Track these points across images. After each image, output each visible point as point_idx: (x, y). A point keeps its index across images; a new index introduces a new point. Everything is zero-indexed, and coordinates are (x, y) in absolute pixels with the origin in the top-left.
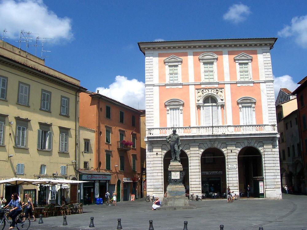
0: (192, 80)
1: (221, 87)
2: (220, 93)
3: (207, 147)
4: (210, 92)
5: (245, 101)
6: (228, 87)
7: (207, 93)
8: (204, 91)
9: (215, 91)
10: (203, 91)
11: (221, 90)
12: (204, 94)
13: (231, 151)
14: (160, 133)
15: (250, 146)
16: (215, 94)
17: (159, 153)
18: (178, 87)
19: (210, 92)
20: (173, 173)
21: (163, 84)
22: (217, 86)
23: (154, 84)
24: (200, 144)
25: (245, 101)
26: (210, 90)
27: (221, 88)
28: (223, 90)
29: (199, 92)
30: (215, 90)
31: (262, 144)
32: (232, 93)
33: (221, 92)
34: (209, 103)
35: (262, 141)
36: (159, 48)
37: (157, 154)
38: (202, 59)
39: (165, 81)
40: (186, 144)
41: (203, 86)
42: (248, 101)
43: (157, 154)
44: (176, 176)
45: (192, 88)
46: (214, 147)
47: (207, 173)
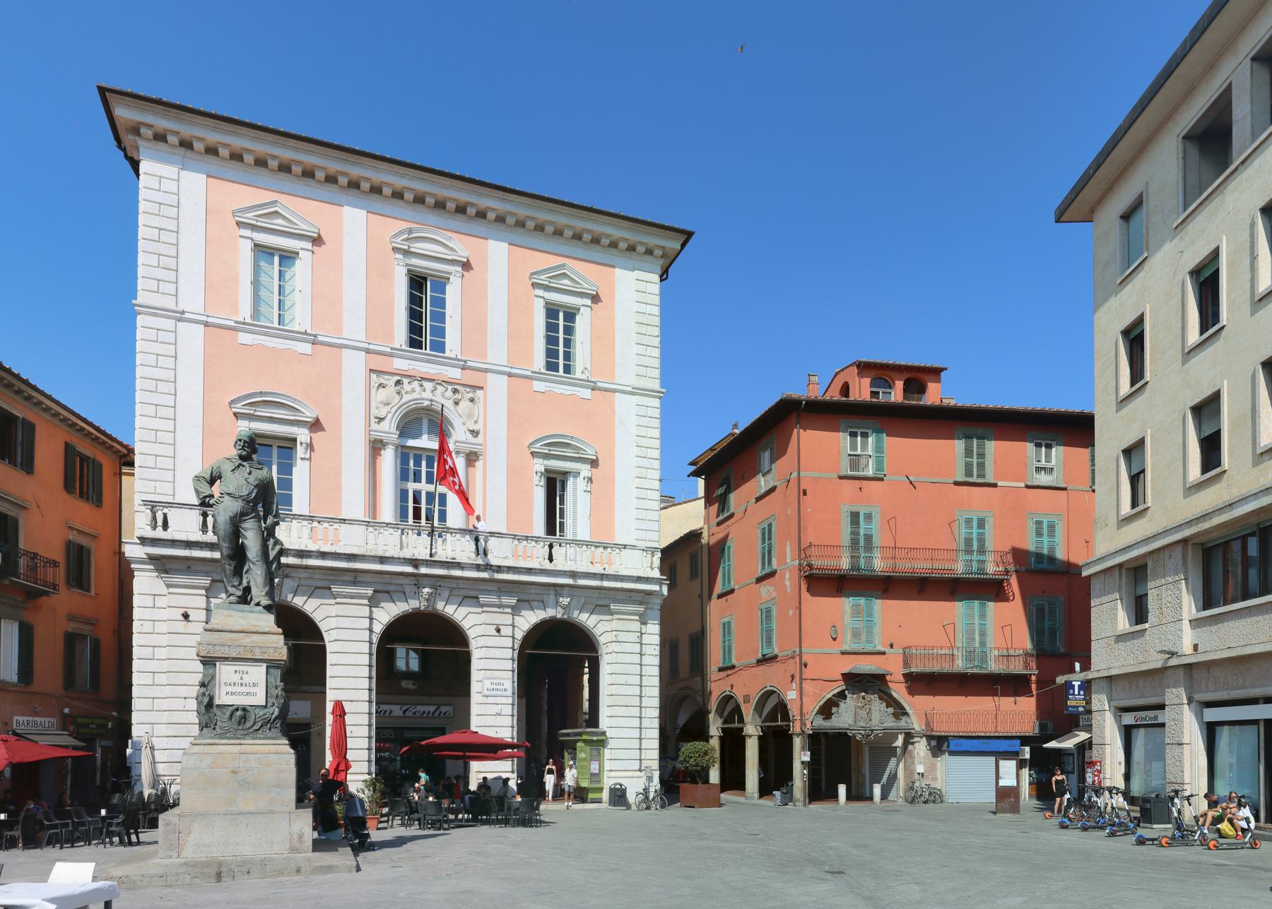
2: (464, 404)
5: (556, 451)
6: (497, 387)
7: (415, 396)
8: (406, 385)
9: (449, 393)
10: (398, 383)
11: (471, 395)
12: (406, 398)
13: (498, 631)
16: (449, 404)
19: (428, 395)
22: (455, 374)
23: (180, 308)
25: (556, 451)
26: (428, 386)
28: (479, 393)
29: (381, 386)
30: (450, 388)
32: (511, 413)
33: (472, 400)
38: (407, 253)
39: (235, 307)
45: (354, 365)
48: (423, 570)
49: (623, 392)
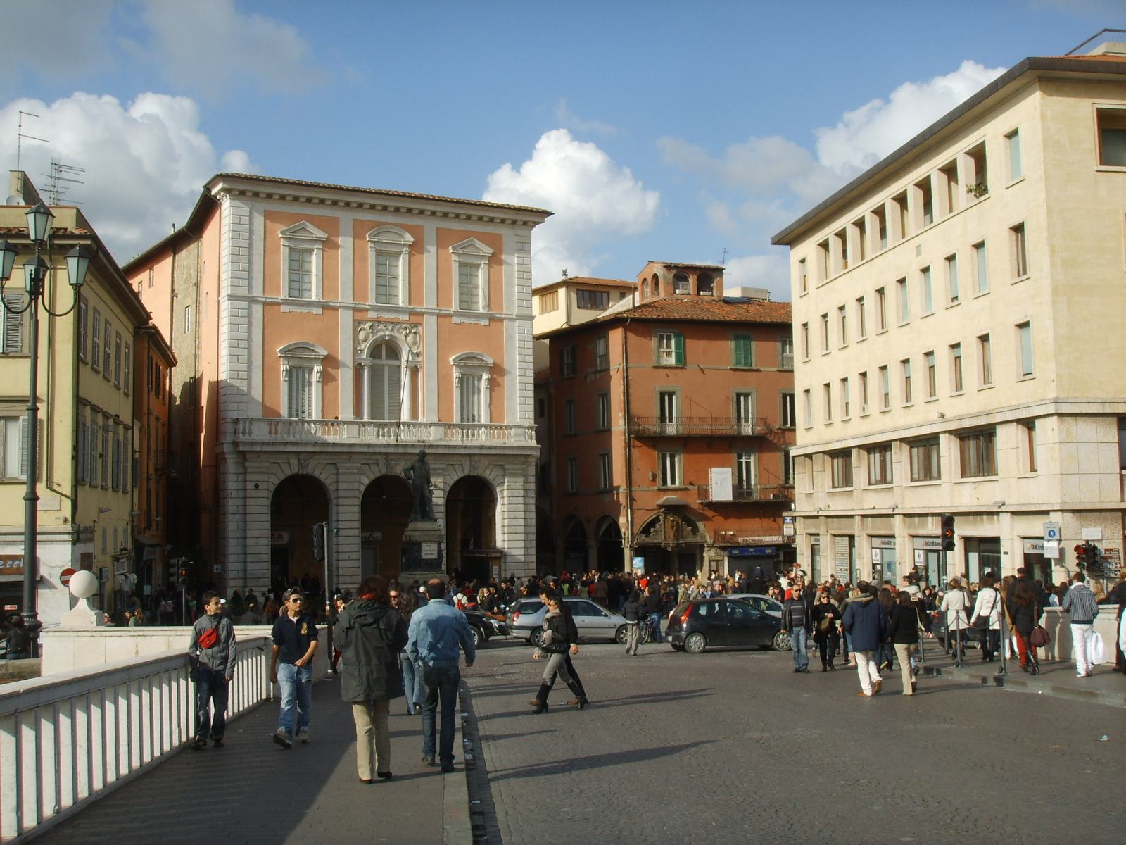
0: (344, 296)
1: (415, 317)
3: (378, 474)
4: (386, 333)
6: (429, 326)
7: (381, 334)
14: (270, 432)
15: (476, 474)
17: (262, 486)
18: (312, 311)
20: (424, 547)
21: (271, 297)
24: (362, 464)
27: (416, 325)
28: (420, 329)
31: (501, 472)
34: (380, 357)
35: (501, 463)
36: (270, 196)
37: (257, 486)
40: (327, 464)
41: (371, 315)
42: (477, 363)
43: (257, 486)
44: (430, 553)
46: (393, 474)
47: (367, 535)
48: (391, 450)
49: (510, 319)
